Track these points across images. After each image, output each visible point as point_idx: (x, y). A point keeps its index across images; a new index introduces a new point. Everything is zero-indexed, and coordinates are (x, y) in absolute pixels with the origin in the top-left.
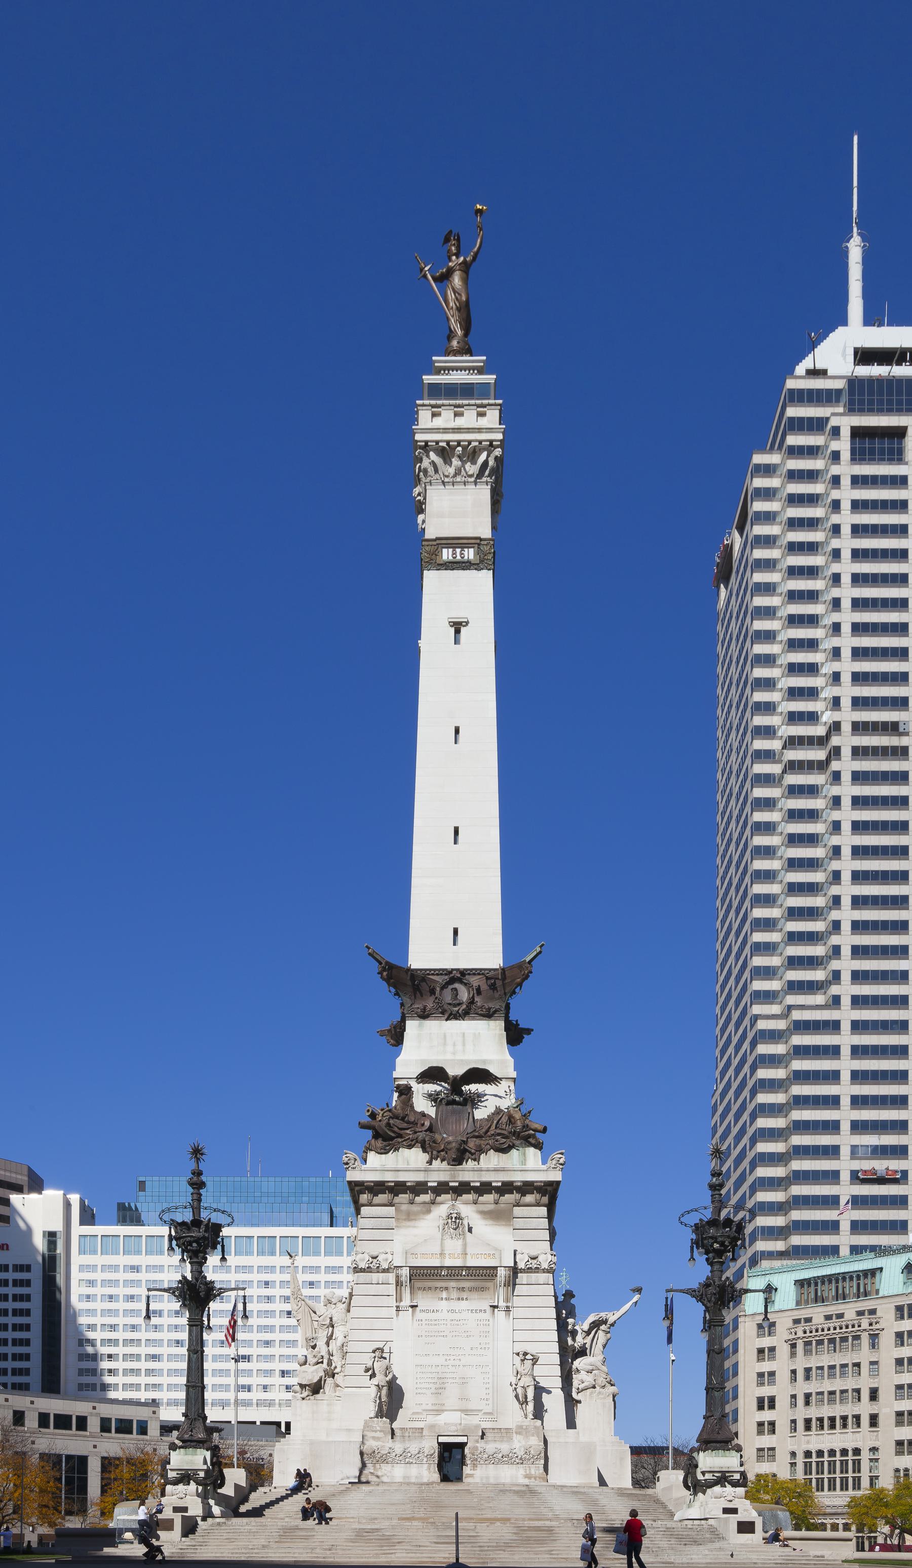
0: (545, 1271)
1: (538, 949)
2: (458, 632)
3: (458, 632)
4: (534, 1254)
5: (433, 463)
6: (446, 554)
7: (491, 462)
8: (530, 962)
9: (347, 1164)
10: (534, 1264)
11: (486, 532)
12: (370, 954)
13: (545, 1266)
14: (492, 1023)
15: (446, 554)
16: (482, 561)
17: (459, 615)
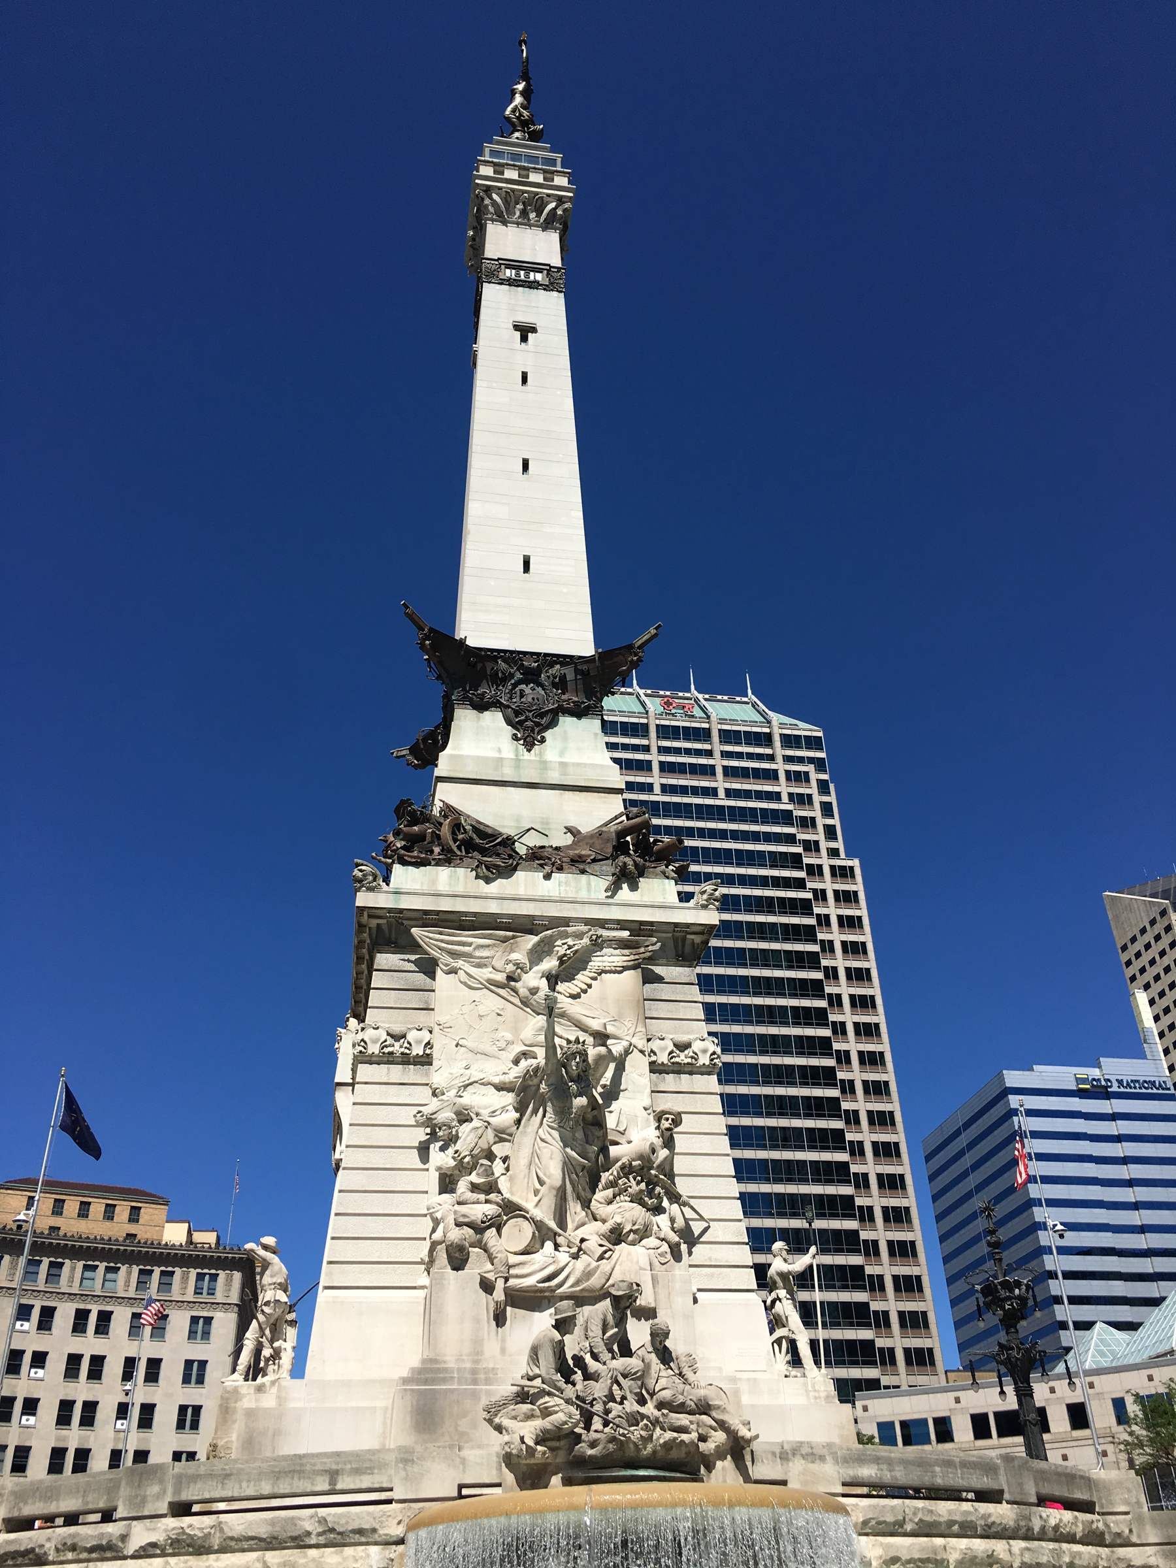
0: (705, 1071)
1: (653, 631)
2: (524, 339)
3: (524, 339)
4: (683, 1038)
5: (494, 203)
6: (509, 273)
7: (559, 212)
8: (639, 648)
9: (360, 881)
10: (683, 1058)
11: (556, 261)
12: (407, 614)
13: (704, 1060)
14: (585, 722)
15: (509, 273)
16: (552, 284)
17: (525, 318)
